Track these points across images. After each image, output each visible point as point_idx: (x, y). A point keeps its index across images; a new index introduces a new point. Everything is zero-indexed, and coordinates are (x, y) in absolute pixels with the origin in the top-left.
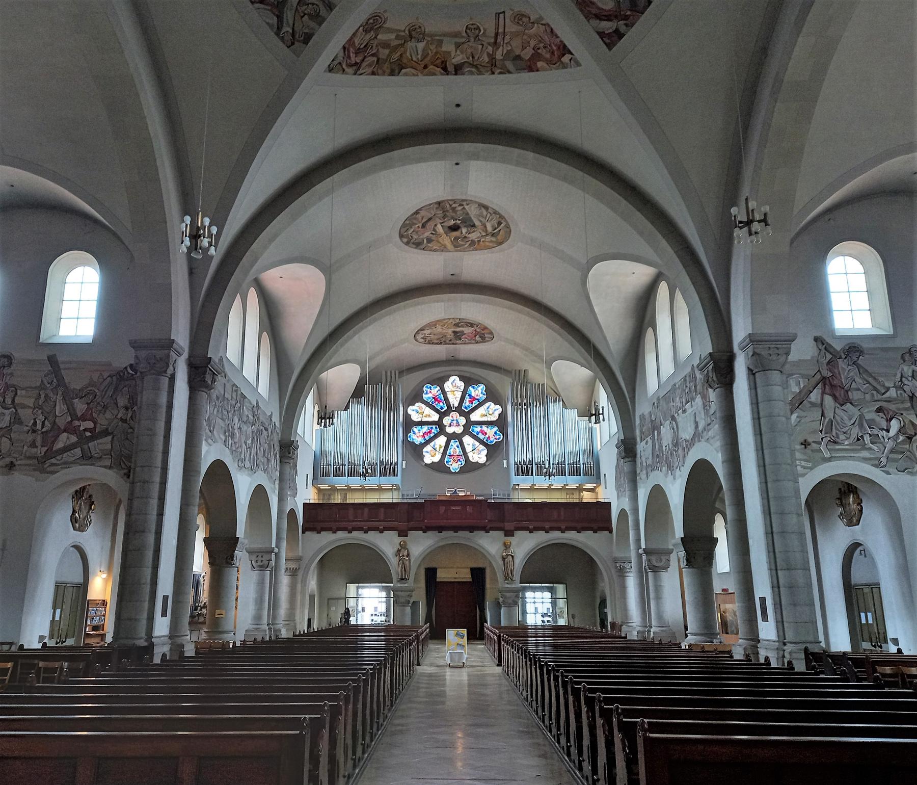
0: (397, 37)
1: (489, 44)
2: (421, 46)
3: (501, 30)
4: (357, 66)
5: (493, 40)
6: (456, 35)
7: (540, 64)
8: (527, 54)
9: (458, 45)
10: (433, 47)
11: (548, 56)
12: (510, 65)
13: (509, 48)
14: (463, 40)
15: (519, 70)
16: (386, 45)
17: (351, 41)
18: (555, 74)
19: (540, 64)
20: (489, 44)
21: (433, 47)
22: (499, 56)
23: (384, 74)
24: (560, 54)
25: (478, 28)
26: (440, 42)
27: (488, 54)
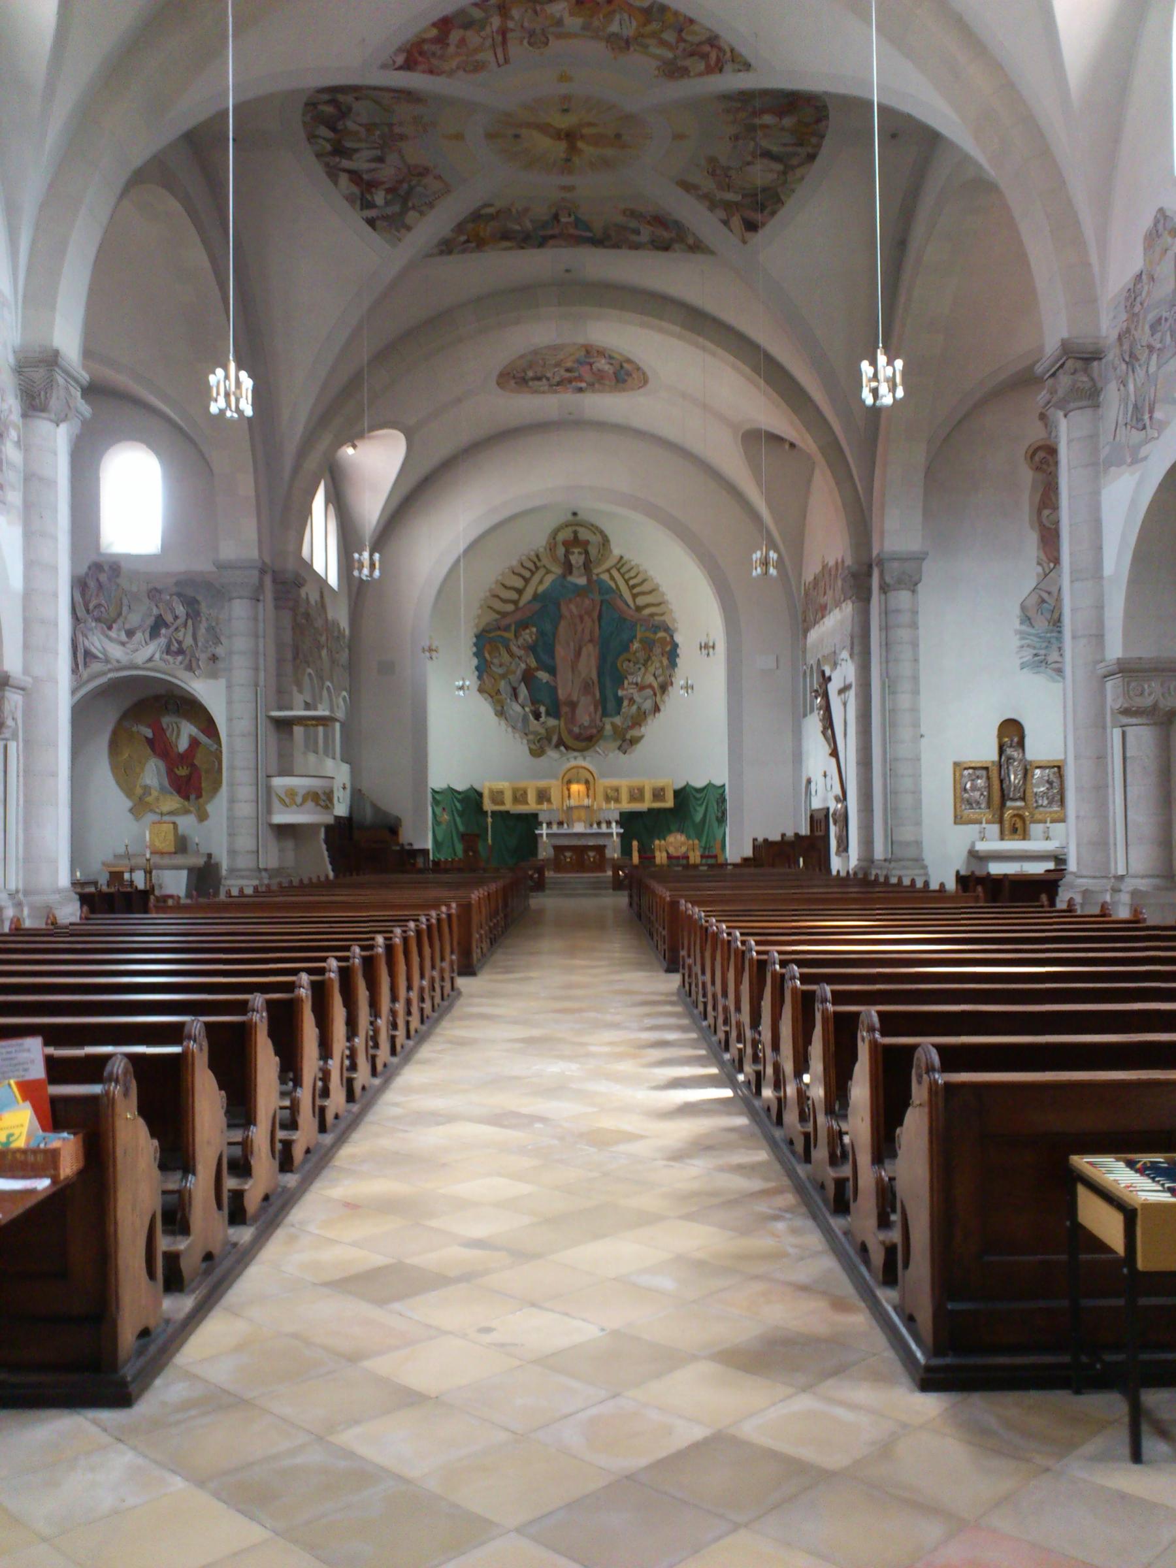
0: (647, 47)
1: (512, 30)
2: (614, 28)
3: (499, 51)
4: (713, 41)
5: (509, 35)
6: (559, 36)
7: (434, 32)
8: (455, 36)
9: (559, 22)
10: (596, 23)
11: (426, 47)
12: (477, 14)
13: (483, 33)
14: (552, 29)
15: (462, 12)
16: (663, 43)
17: (709, 70)
18: (408, 34)
19: (434, 32)
20: (512, 30)
21: (596, 23)
22: (496, 22)
23: (676, 14)
24: (414, 56)
25: (530, 44)
26: (585, 28)
27: (512, 18)
